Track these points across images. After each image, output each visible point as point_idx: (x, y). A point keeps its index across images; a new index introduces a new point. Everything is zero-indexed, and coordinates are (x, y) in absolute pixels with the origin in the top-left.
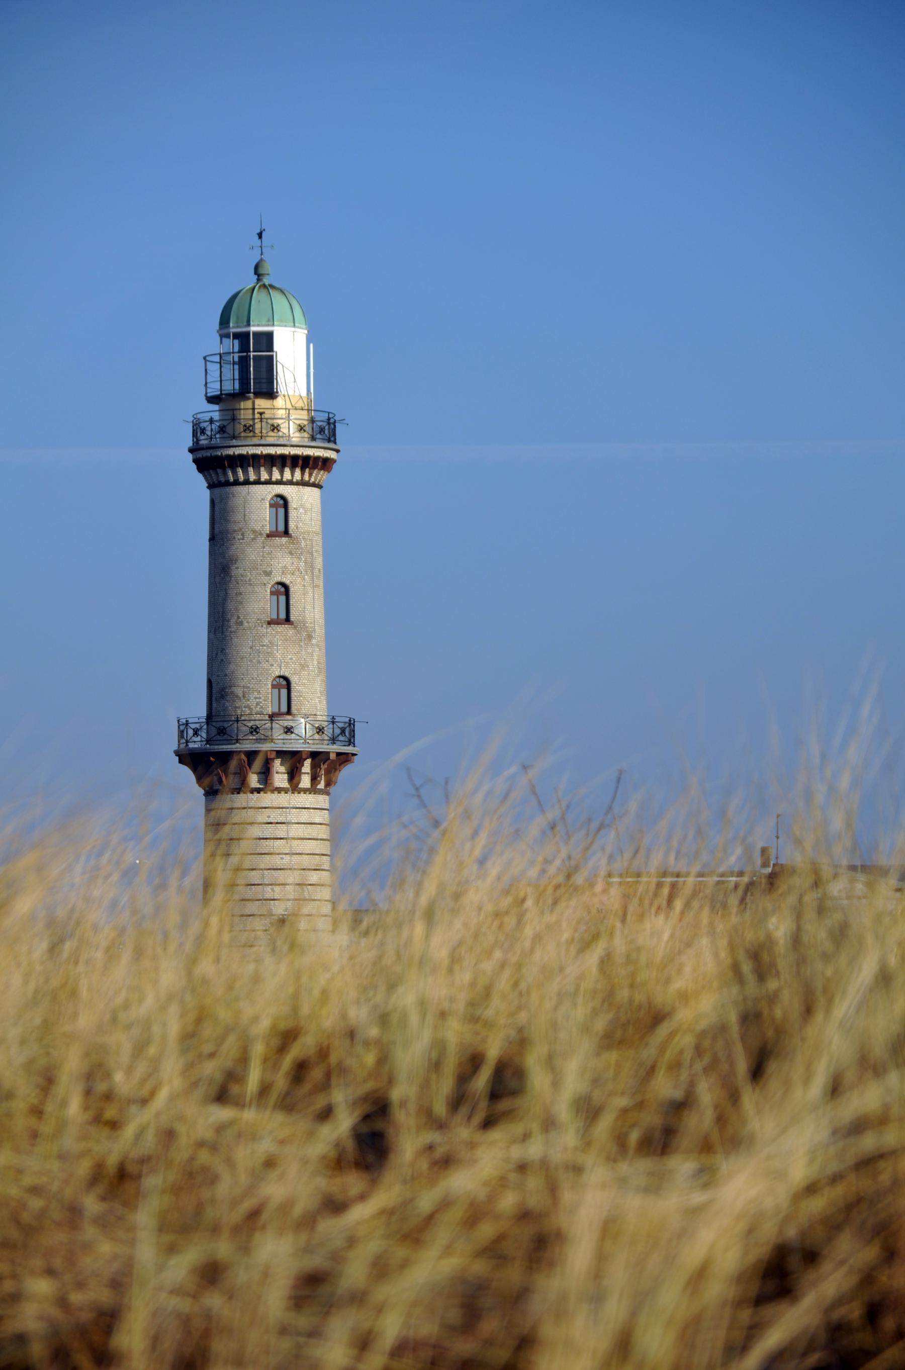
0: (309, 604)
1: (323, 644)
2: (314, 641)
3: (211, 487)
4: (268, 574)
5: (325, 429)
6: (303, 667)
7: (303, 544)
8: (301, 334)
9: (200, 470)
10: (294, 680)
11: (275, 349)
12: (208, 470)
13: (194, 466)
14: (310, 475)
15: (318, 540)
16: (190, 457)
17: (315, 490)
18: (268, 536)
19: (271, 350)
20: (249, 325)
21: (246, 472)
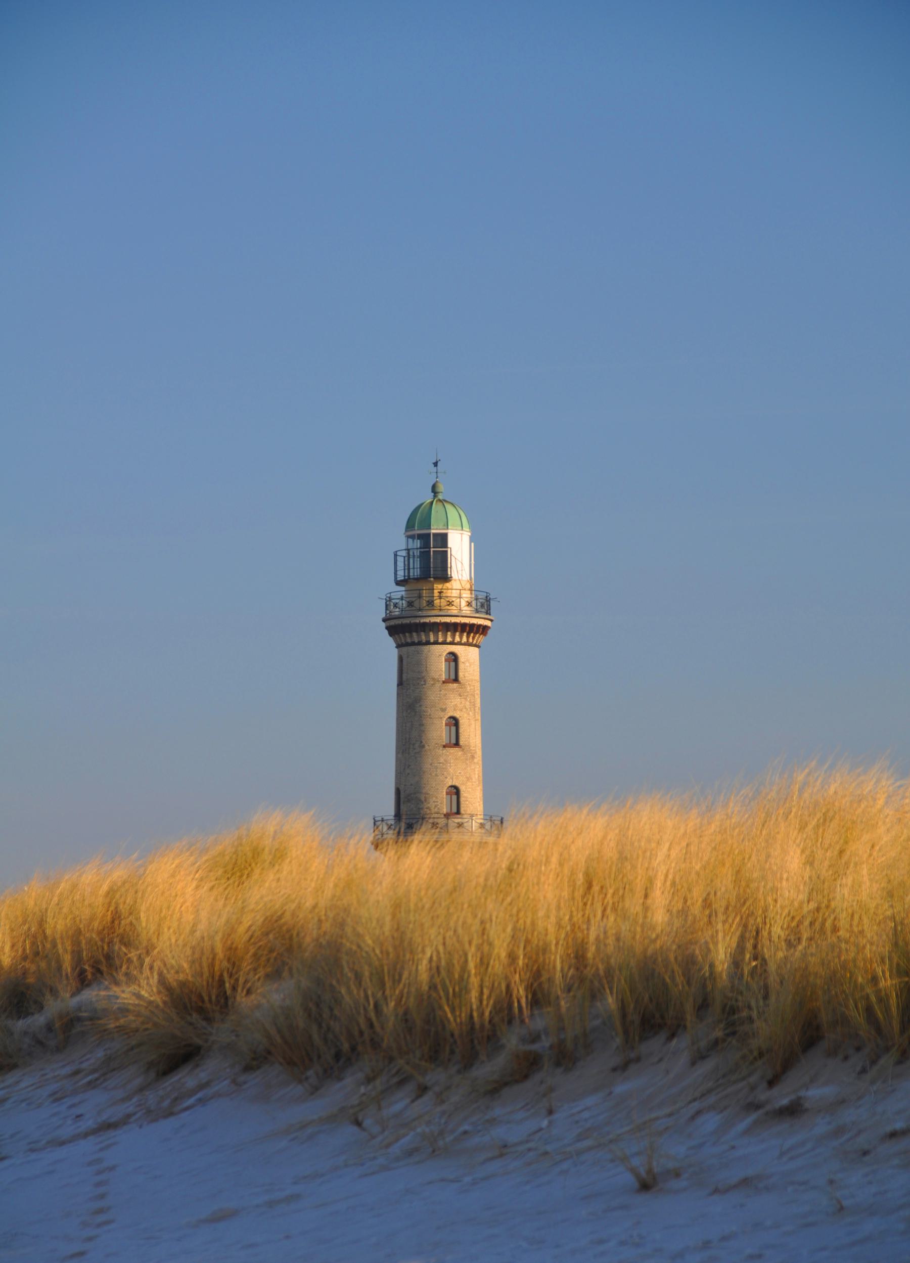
0: (472, 733)
1: (480, 762)
2: (476, 760)
3: (398, 646)
4: (444, 710)
5: (484, 605)
6: (469, 779)
7: (468, 688)
8: (466, 536)
9: (391, 634)
10: (462, 789)
11: (449, 546)
12: (398, 634)
13: (386, 632)
14: (473, 638)
15: (478, 685)
16: (383, 625)
17: (477, 649)
18: (444, 682)
19: (446, 546)
20: (430, 528)
21: (419, 636)
